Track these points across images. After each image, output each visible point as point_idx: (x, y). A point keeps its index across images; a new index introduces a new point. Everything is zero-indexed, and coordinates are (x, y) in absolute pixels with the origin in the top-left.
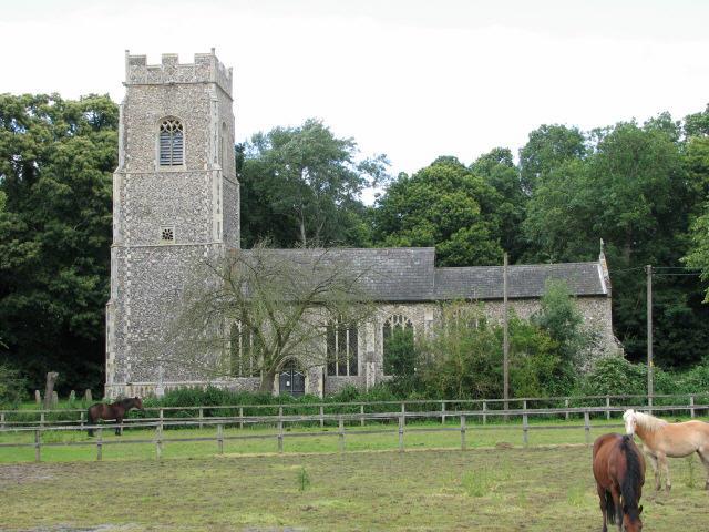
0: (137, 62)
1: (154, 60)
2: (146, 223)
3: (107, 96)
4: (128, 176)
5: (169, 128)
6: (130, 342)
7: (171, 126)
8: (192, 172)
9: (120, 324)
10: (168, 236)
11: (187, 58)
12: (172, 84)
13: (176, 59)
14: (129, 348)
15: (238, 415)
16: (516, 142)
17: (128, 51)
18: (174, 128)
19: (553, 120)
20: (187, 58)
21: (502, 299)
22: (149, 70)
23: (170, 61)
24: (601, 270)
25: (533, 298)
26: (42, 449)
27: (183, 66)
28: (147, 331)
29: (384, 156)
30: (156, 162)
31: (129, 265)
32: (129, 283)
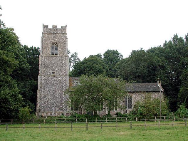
0: (45, 27)
1: (50, 27)
2: (48, 69)
3: (151, 48)
4: (43, 57)
5: (54, 45)
6: (43, 101)
7: (55, 44)
8: (60, 56)
9: (41, 96)
10: (54, 73)
11: (59, 27)
12: (55, 33)
13: (56, 27)
14: (43, 103)
15: (11, 121)
16: (102, 52)
17: (43, 24)
18: (55, 45)
19: (112, 48)
20: (59, 27)
21: (159, 92)
22: (49, 29)
23: (55, 27)
24: (159, 85)
25: (150, 92)
26: (73, 129)
27: (58, 29)
28: (48, 98)
29: (76, 53)
30: (51, 54)
31: (43, 81)
32: (43, 85)
